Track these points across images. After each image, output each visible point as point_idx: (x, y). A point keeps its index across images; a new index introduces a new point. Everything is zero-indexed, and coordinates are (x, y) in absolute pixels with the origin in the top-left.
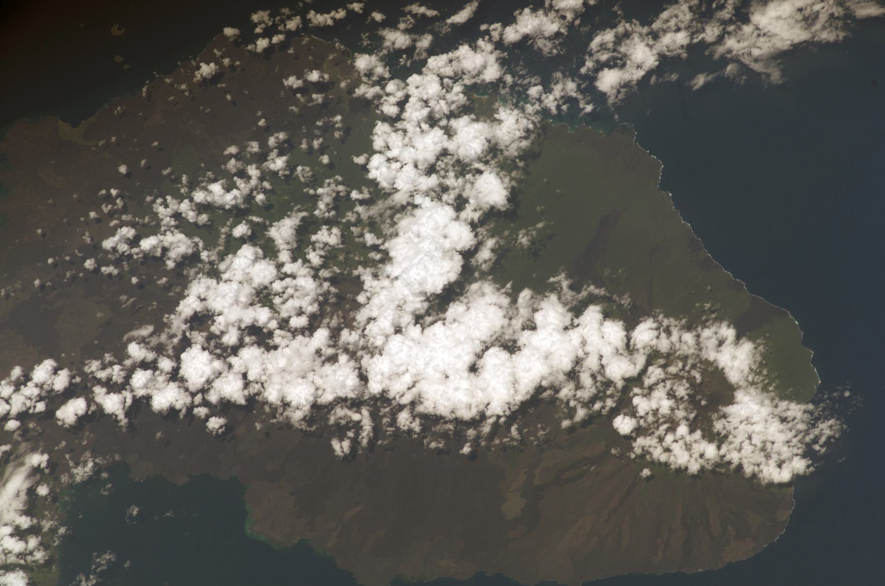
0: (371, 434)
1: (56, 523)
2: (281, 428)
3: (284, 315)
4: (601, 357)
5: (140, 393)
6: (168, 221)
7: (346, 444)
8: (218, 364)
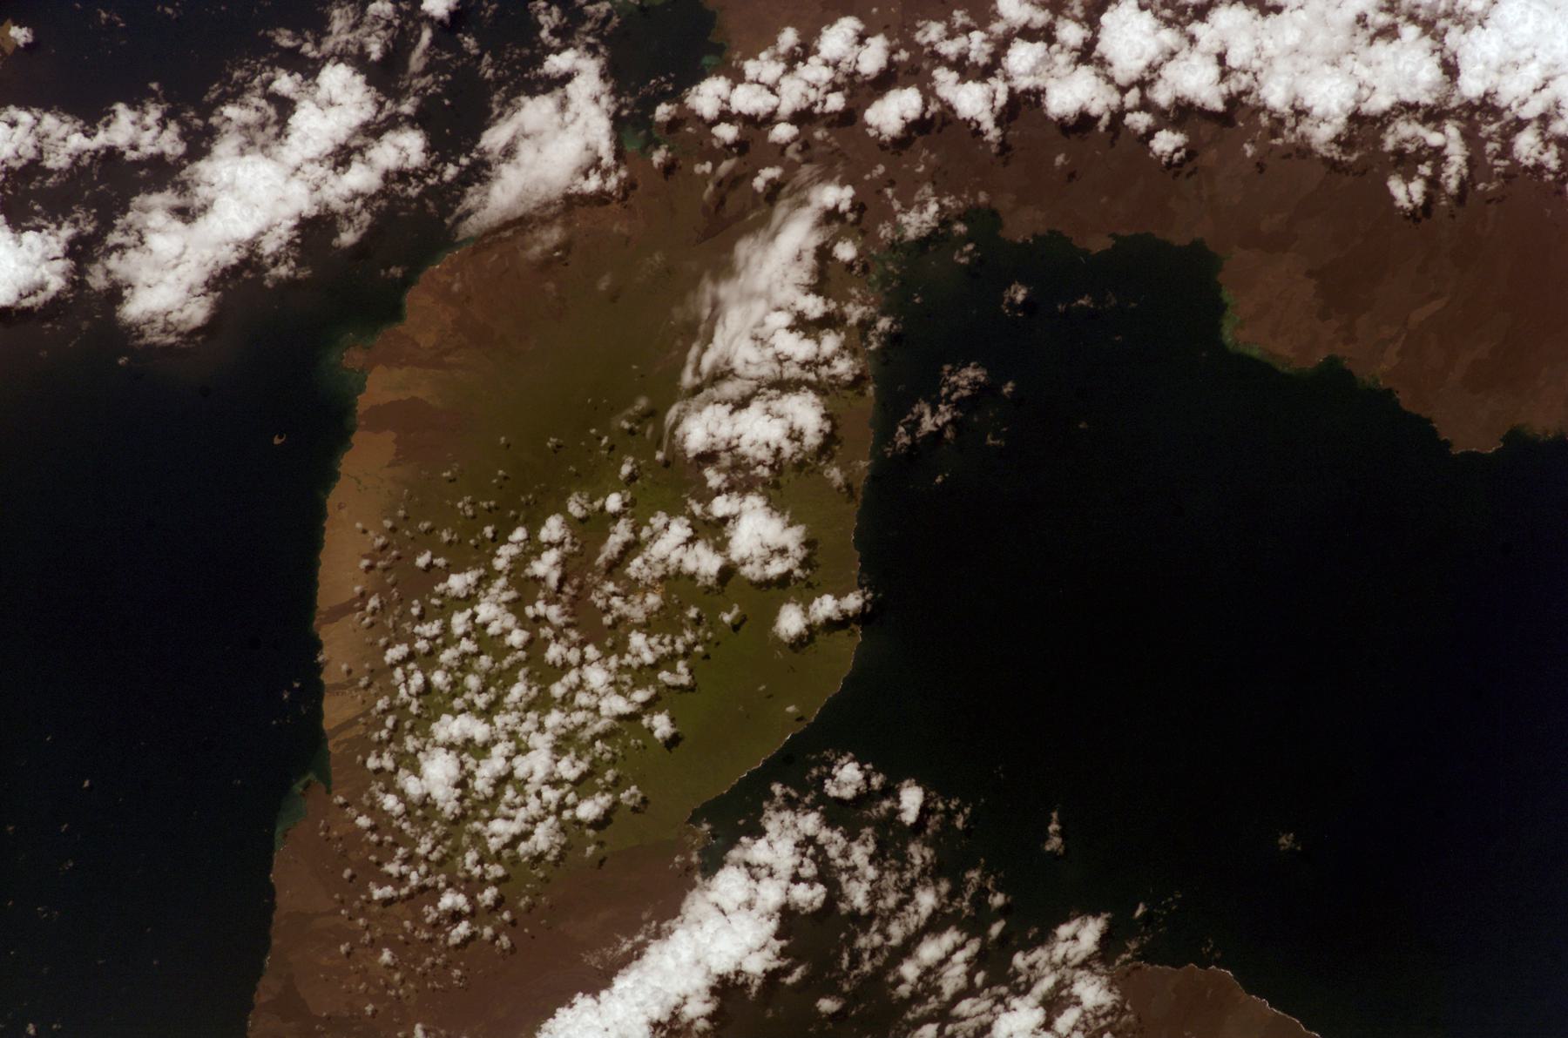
0: (1465, 171)
1: (872, 310)
2: (1289, 156)
7: (1417, 187)
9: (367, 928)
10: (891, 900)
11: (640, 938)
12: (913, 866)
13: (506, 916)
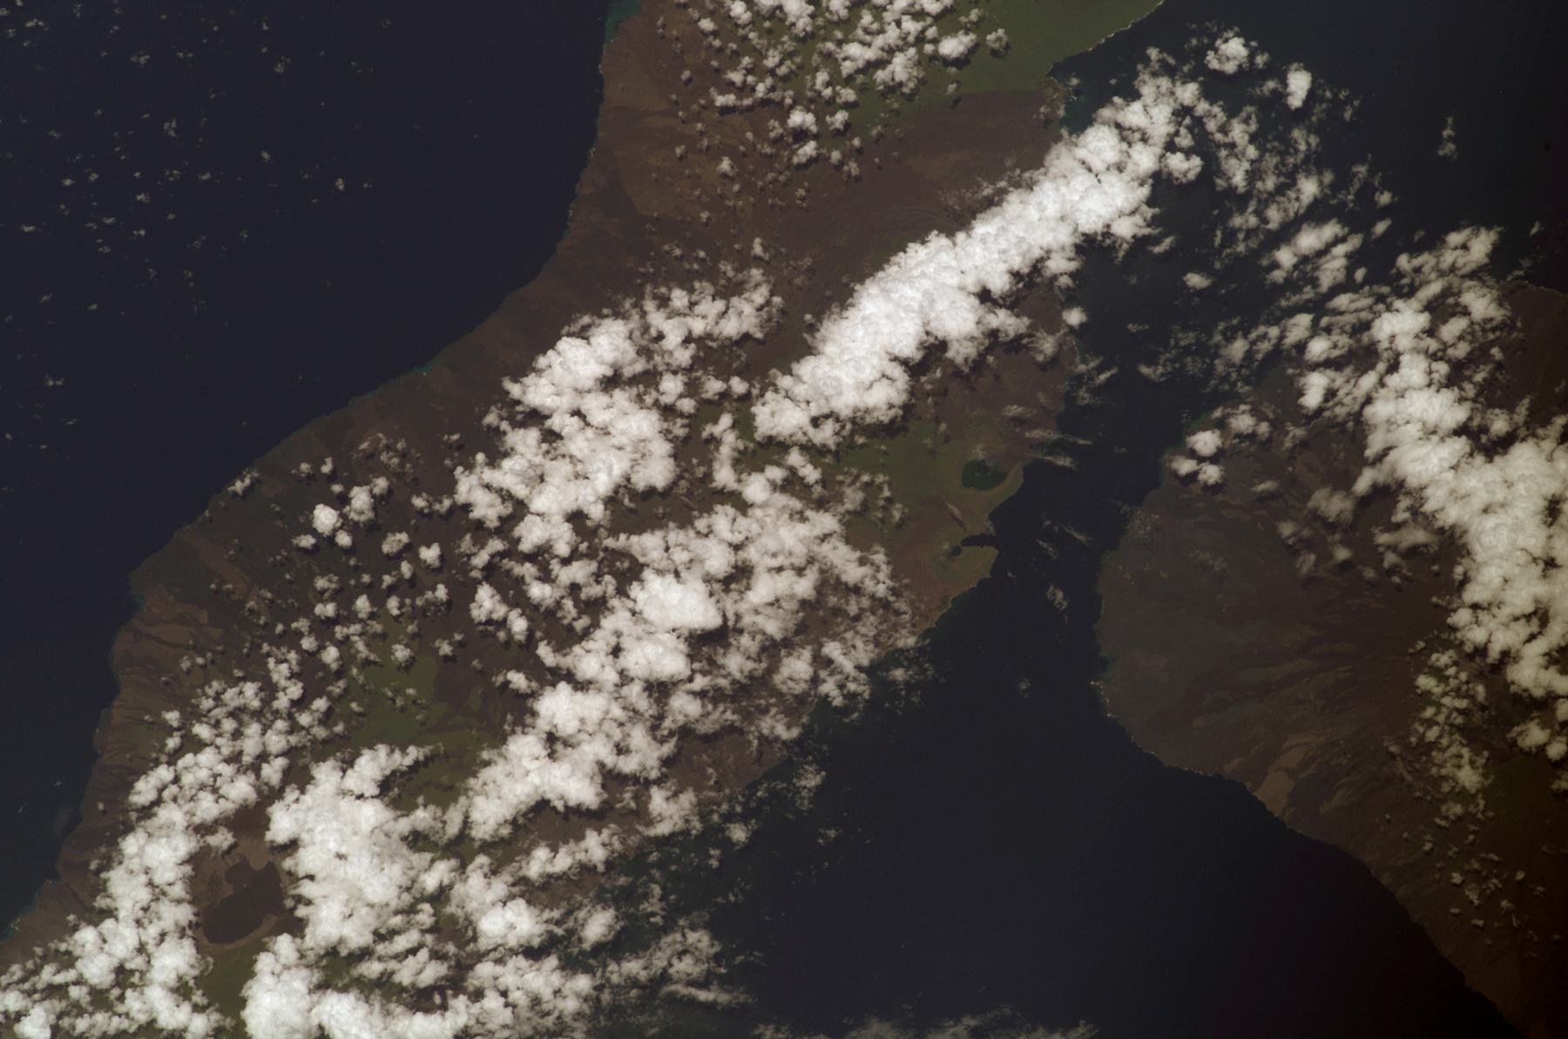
9: (702, 133)
10: (1270, 183)
11: (1002, 184)
12: (1297, 151)
13: (856, 142)
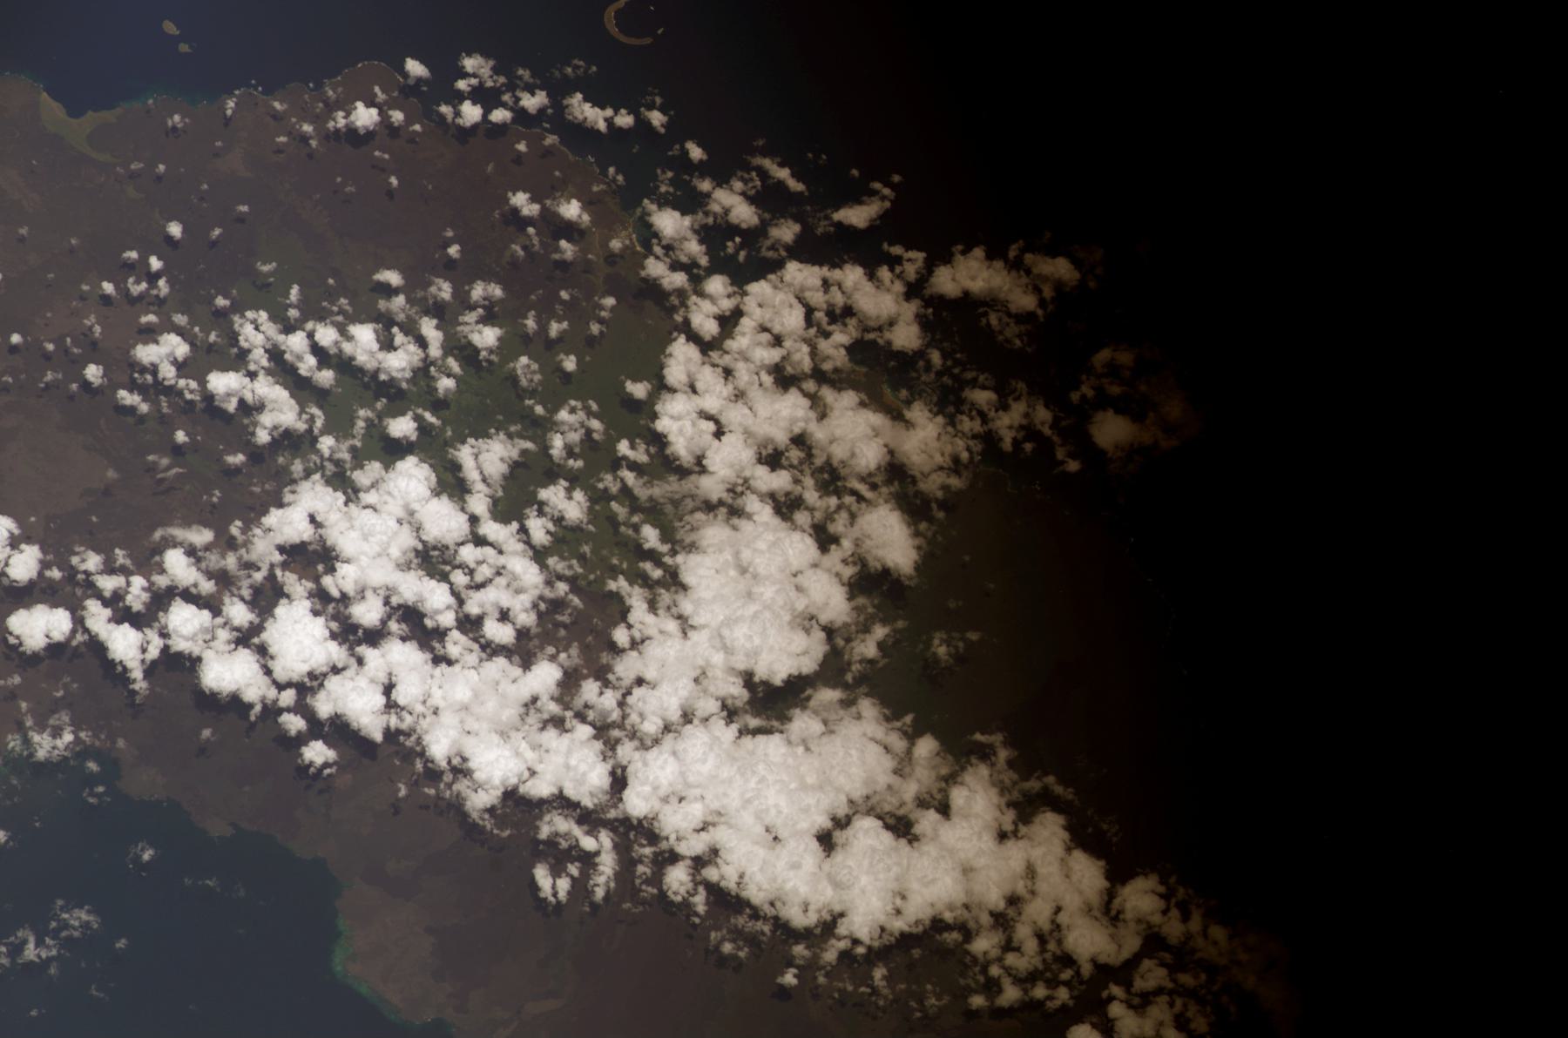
0: (612, 885)
2: (427, 808)
3: (473, 608)
4: (1058, 910)
5: (180, 645)
6: (259, 357)
7: (564, 885)
8: (336, 652)
